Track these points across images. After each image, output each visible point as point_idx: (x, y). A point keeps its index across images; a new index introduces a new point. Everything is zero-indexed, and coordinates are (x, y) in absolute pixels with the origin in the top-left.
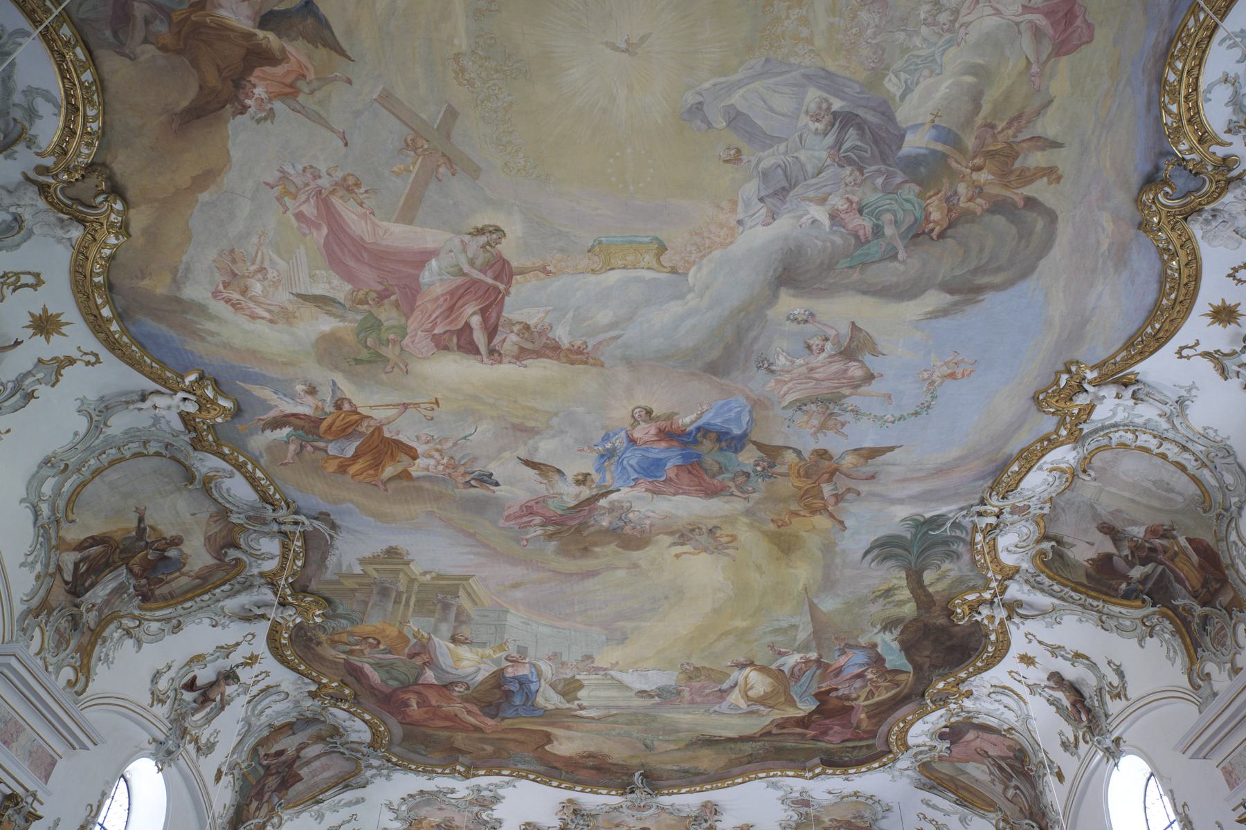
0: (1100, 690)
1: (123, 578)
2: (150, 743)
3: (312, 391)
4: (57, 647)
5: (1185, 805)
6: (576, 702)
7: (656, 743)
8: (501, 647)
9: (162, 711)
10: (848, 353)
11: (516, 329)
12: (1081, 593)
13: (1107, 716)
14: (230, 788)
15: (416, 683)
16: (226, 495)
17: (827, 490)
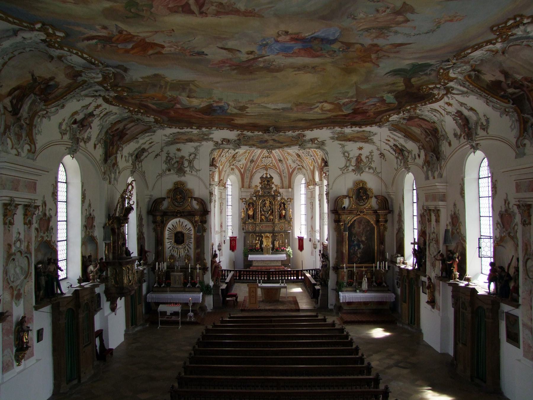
0: (476, 123)
1: (33, 98)
2: (66, 150)
3: (105, 28)
4: (18, 141)
5: (496, 181)
8: (211, 98)
9: (66, 137)
10: (398, 13)
11: (215, 4)
12: (482, 91)
13: (476, 134)
14: (100, 148)
16: (70, 61)
17: (373, 56)
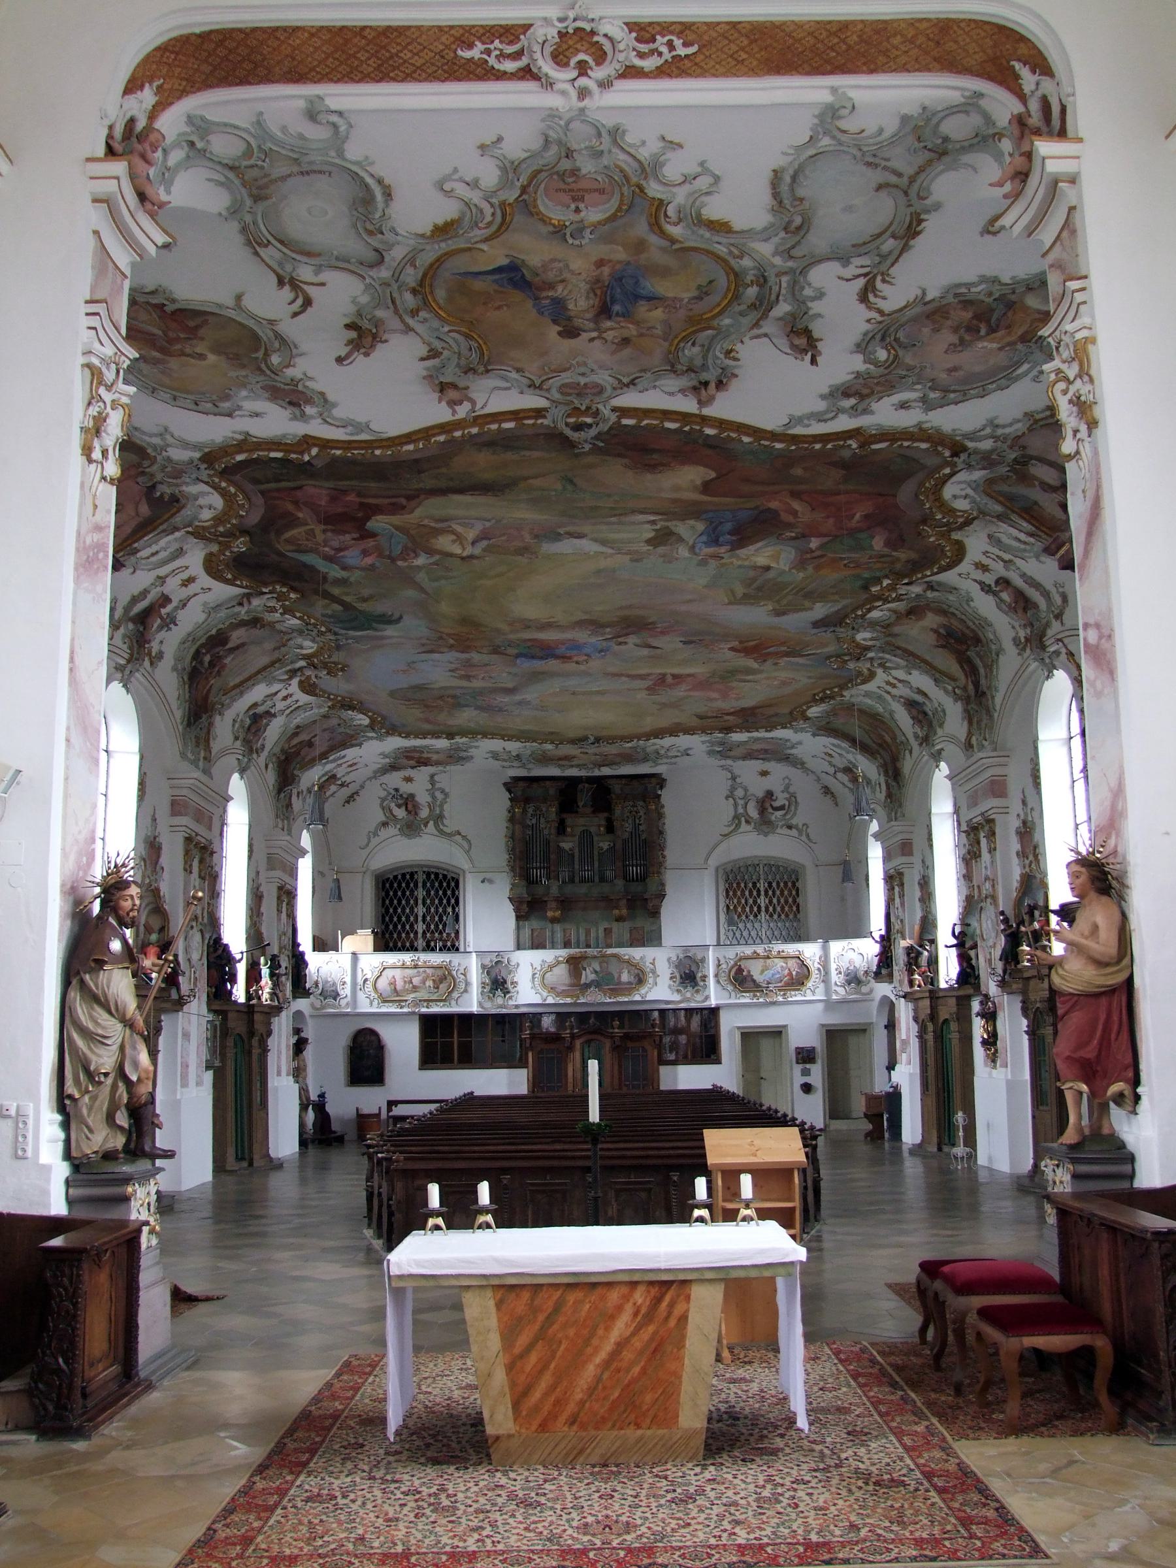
6: (658, 527)
7: (559, 486)
8: (723, 565)
15: (836, 536)
17: (452, 642)
